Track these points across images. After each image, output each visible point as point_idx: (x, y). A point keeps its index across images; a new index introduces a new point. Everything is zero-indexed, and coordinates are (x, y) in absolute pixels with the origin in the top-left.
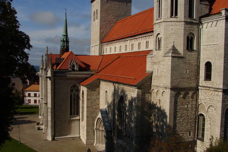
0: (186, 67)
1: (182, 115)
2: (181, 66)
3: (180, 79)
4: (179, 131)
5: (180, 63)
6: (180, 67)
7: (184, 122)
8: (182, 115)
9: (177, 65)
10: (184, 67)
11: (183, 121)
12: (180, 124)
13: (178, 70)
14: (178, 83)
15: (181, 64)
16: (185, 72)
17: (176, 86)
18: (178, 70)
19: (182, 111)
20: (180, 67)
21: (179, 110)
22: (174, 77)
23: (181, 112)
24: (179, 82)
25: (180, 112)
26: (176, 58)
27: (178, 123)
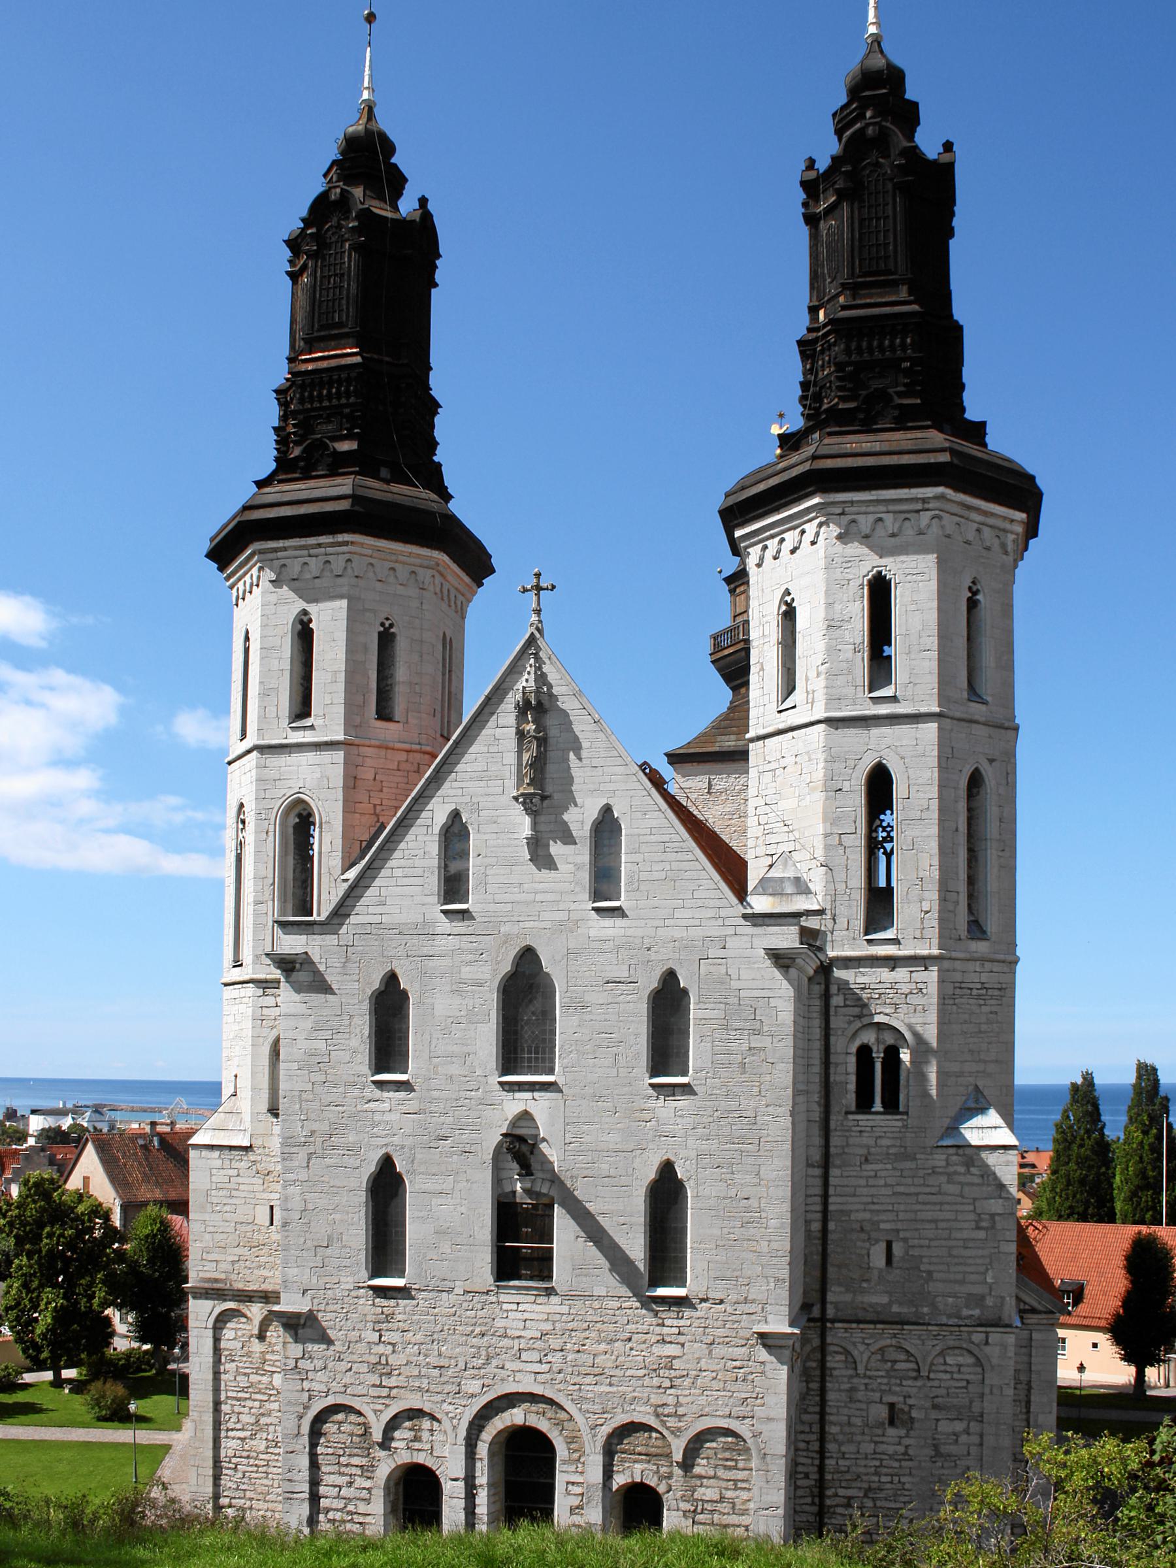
0: (265, 1196)
1: (263, 1420)
2: (242, 1187)
3: (239, 1251)
4: (248, 1494)
5: (238, 1175)
6: (234, 1193)
7: (273, 1457)
8: (263, 1420)
9: (219, 1186)
10: (259, 1196)
11: (267, 1447)
12: (252, 1461)
13: (227, 1208)
14: (224, 1266)
15: (240, 1180)
16: (263, 1216)
17: (216, 1280)
18: (227, 1208)
19: (261, 1401)
20: (234, 1193)
21: (247, 1395)
22: (207, 1236)
23: (257, 1404)
24: (233, 1262)
25: (249, 1403)
26: (217, 1153)
27: (245, 1454)
